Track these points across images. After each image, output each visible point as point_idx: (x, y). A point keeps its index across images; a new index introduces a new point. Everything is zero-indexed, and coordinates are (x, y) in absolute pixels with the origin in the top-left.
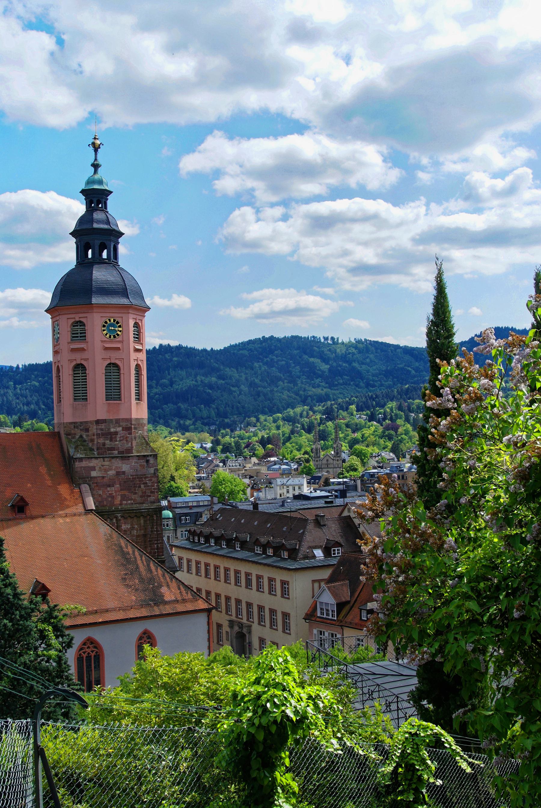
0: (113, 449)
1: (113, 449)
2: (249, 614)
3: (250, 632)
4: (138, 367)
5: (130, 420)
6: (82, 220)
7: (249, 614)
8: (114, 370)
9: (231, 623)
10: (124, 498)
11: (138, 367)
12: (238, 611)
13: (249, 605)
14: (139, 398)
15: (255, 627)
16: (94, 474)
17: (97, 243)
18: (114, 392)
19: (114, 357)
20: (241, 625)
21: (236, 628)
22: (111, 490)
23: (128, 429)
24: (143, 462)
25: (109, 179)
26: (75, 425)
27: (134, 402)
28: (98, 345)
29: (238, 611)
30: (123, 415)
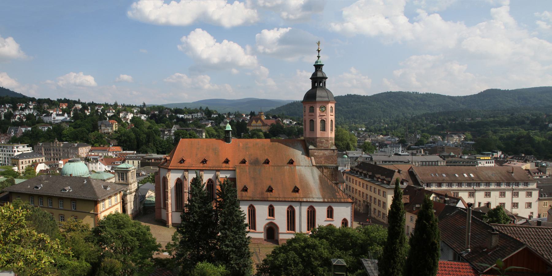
0: (322, 146)
1: (322, 146)
2: (371, 200)
3: (370, 205)
4: (332, 120)
5: (328, 138)
6: (314, 75)
7: (371, 200)
8: (323, 122)
9: (364, 201)
10: (325, 162)
11: (332, 120)
12: (367, 198)
13: (371, 197)
14: (332, 130)
15: (373, 204)
16: (315, 154)
17: (319, 81)
18: (324, 129)
19: (323, 118)
20: (368, 203)
21: (366, 203)
22: (322, 159)
23: (327, 141)
24: (332, 151)
25: (322, 61)
26: (310, 138)
27: (330, 132)
28: (318, 114)
29: (367, 198)
30: (326, 136)
